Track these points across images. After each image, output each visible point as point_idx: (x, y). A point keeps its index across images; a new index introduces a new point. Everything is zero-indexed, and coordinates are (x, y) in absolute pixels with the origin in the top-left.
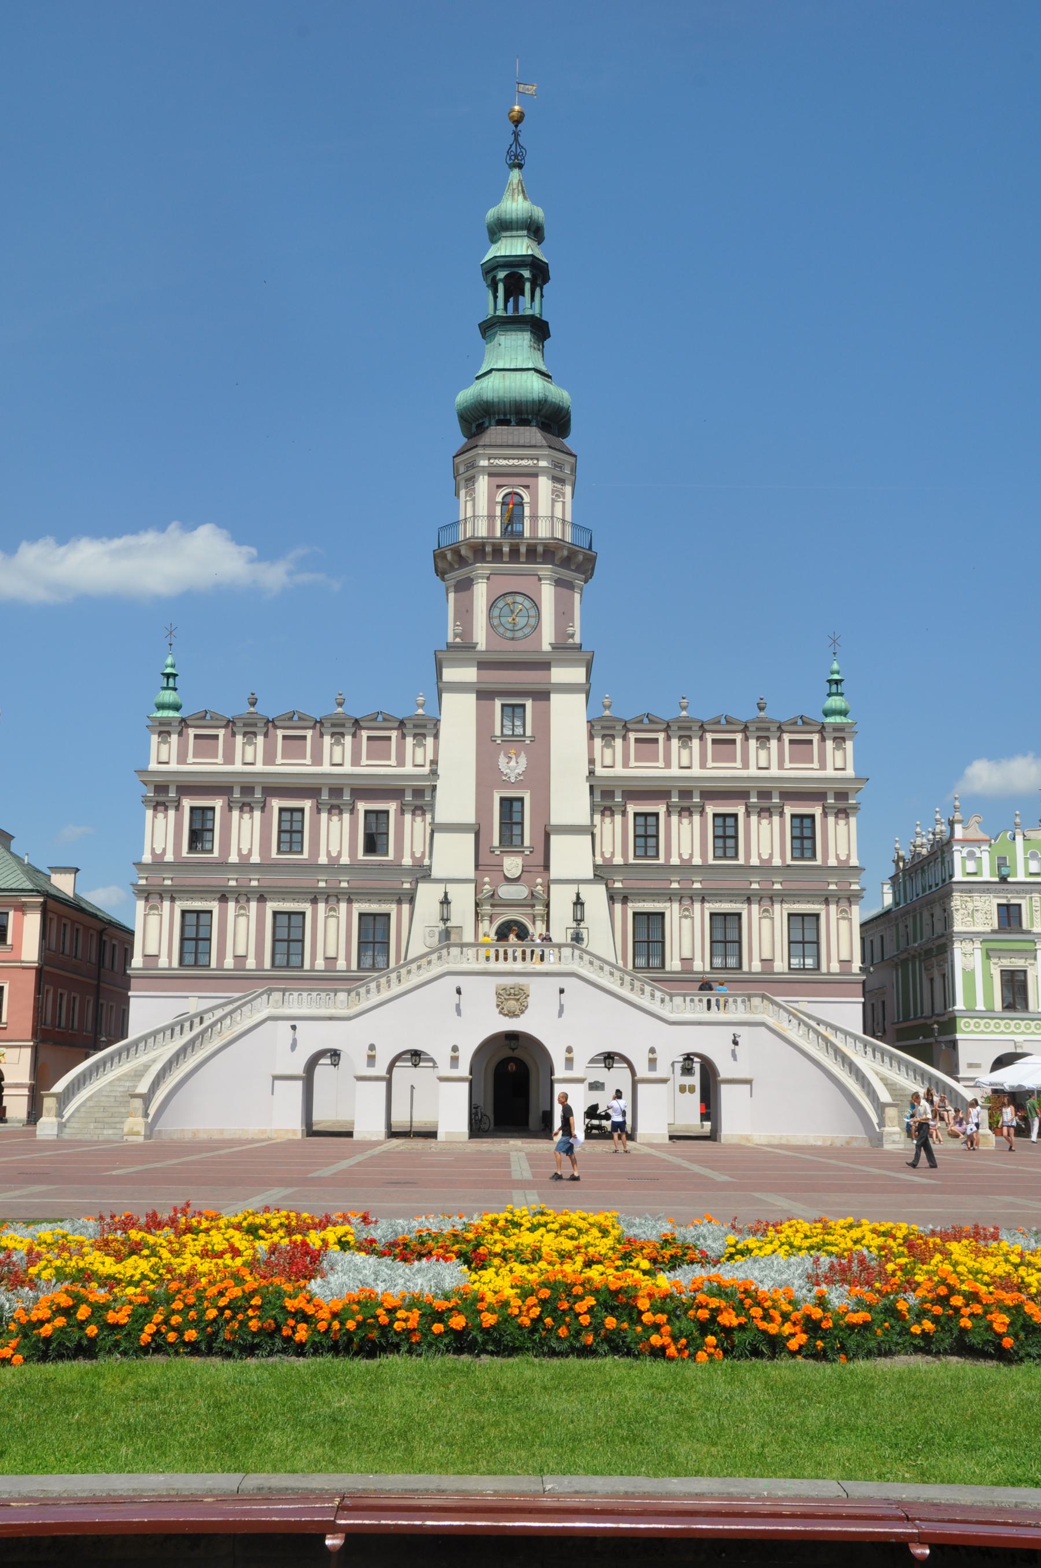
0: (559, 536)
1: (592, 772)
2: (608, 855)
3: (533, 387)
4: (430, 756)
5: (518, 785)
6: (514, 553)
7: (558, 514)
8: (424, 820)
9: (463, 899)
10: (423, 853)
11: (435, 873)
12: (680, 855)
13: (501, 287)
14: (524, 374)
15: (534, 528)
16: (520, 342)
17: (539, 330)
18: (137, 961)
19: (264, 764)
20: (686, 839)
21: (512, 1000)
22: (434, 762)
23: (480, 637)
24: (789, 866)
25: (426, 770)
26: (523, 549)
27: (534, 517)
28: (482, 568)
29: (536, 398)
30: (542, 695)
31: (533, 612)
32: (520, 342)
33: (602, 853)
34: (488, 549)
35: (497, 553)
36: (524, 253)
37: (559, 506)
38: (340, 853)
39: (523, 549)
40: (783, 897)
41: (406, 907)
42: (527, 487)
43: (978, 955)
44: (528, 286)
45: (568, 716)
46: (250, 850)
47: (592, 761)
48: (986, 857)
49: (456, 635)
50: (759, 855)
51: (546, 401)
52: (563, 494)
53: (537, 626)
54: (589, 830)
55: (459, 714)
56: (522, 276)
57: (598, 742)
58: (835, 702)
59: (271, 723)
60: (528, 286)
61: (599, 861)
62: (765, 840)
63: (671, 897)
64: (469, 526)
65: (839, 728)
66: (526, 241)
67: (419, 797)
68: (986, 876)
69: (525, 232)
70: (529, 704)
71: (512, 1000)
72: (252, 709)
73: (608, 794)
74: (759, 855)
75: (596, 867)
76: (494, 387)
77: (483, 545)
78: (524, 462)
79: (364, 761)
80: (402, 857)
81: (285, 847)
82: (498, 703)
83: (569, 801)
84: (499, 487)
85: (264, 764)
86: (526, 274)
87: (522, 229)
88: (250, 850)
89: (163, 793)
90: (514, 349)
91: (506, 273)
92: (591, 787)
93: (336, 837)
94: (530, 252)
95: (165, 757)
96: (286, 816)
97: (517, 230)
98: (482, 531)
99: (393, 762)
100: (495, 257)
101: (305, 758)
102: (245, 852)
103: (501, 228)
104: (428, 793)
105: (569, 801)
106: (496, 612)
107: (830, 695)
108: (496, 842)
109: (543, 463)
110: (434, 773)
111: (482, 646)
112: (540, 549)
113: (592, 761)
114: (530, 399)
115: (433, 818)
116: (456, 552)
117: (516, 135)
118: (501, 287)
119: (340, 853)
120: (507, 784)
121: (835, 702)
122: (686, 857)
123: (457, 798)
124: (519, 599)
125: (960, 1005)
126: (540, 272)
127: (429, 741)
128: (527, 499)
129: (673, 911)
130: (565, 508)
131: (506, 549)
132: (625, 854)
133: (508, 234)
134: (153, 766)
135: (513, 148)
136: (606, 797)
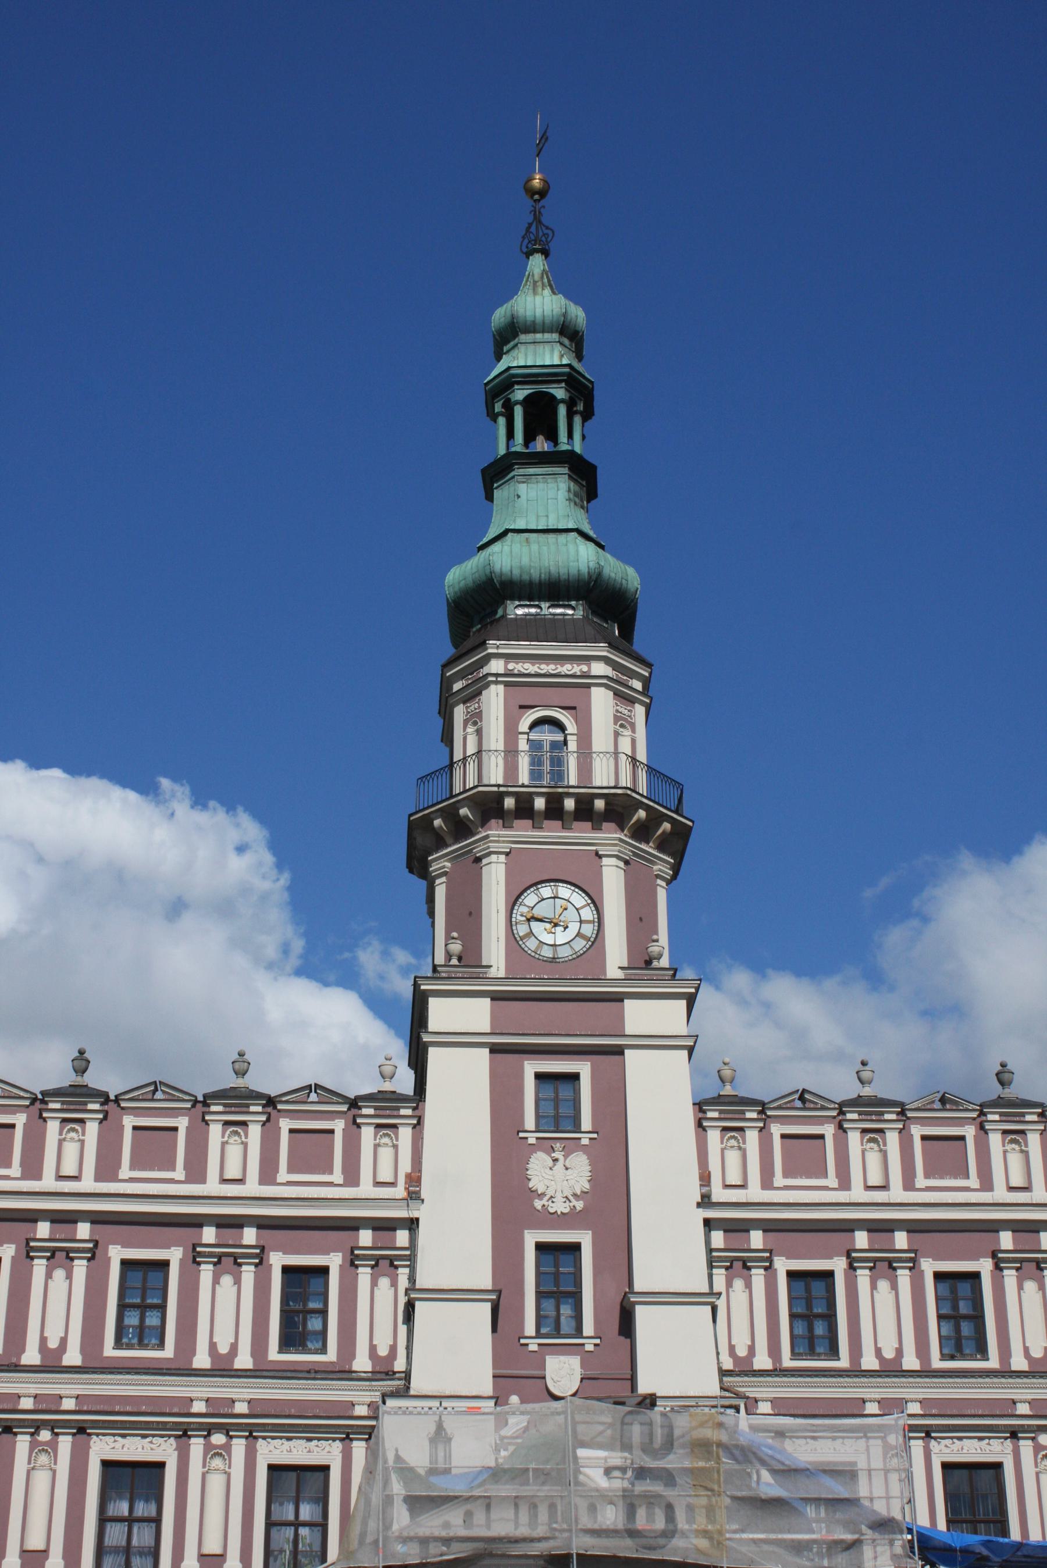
2: (742, 1352)
3: (580, 557)
4: (405, 1166)
6: (555, 811)
8: (394, 1284)
10: (393, 1349)
11: (417, 1385)
12: (878, 1352)
13: (518, 412)
14: (562, 538)
16: (551, 494)
17: (584, 475)
19: (98, 1178)
22: (414, 1179)
23: (495, 954)
25: (400, 1191)
26: (569, 804)
28: (497, 837)
29: (584, 570)
31: (588, 914)
32: (551, 494)
33: (732, 1349)
34: (509, 803)
36: (556, 362)
38: (234, 1348)
39: (569, 804)
41: (359, 1448)
44: (562, 410)
45: (658, 1093)
46: (64, 1341)
47: (705, 1179)
49: (449, 956)
50: (1026, 1350)
51: (600, 574)
54: (709, 1299)
56: (553, 397)
57: (714, 1136)
59: (110, 1104)
60: (562, 410)
61: (728, 1364)
63: (865, 1432)
64: (471, 767)
66: (558, 348)
67: (388, 1241)
69: (555, 336)
70: (584, 1068)
72: (79, 1078)
74: (1026, 1350)
75: (723, 1373)
76: (508, 558)
77: (500, 797)
78: (567, 668)
79: (283, 1176)
80: (353, 1356)
81: (131, 1335)
82: (531, 1067)
84: (524, 707)
85: (98, 1178)
86: (559, 392)
87: (551, 331)
88: (64, 1341)
91: (526, 392)
94: (565, 361)
96: (136, 1278)
98: (495, 774)
99: (337, 1177)
100: (509, 368)
101: (172, 1168)
102: (53, 1344)
104: (402, 1237)
105: (668, 1247)
108: (530, 1328)
109: (599, 669)
110: (414, 1196)
112: (600, 804)
113: (705, 1179)
114: (573, 571)
115: (412, 1279)
116: (450, 813)
118: (518, 412)
119: (234, 1348)
122: (889, 1354)
123: (457, 1242)
124: (564, 891)
126: (582, 393)
127: (405, 1134)
128: (571, 727)
130: (637, 740)
131: (540, 803)
132: (774, 1350)
133: (530, 337)
135: (533, 229)
136: (734, 1239)
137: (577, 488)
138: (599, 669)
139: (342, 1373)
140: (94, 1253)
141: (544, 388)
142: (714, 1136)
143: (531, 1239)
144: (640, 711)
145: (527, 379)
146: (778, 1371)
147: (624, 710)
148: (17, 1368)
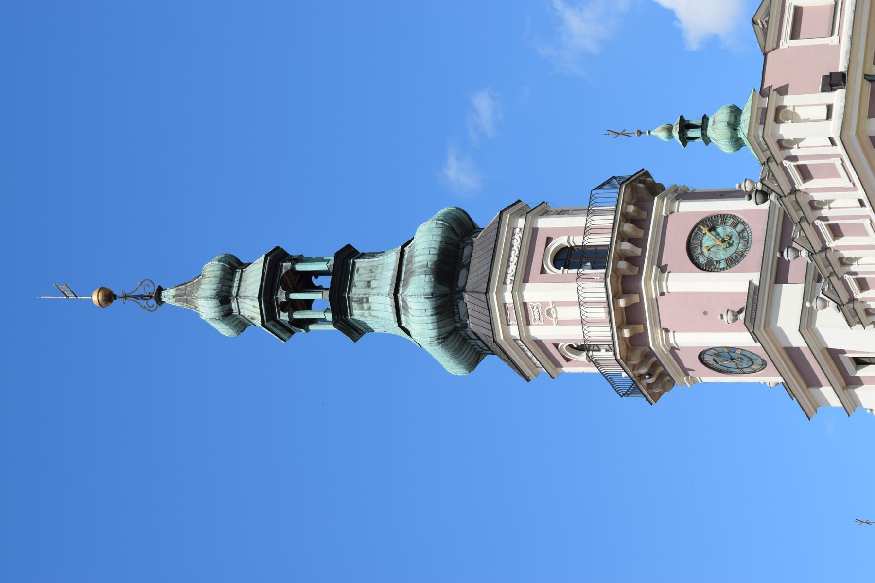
0: (600, 312)
7: (574, 313)
30: (835, 355)
37: (565, 313)
42: (556, 346)
44: (298, 315)
52: (544, 304)
58: (718, 132)
65: (762, 146)
70: (845, 359)
90: (373, 280)
97: (231, 287)
103: (242, 325)
107: (707, 140)
117: (126, 297)
121: (718, 132)
137: (355, 306)
141: (288, 325)
147: (533, 314)
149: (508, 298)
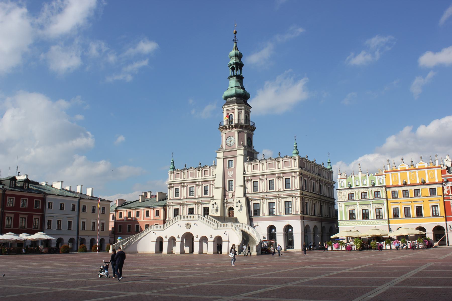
1: (244, 174)
5: (231, 178)
9: (219, 203)
11: (214, 198)
15: (235, 121)
18: (167, 219)
20: (263, 186)
21: (188, 226)
24: (284, 191)
27: (235, 119)
35: (226, 129)
40: (283, 198)
43: (343, 206)
47: (244, 171)
48: (345, 182)
53: (235, 143)
55: (220, 163)
62: (280, 184)
63: (260, 199)
68: (345, 187)
70: (233, 159)
71: (188, 226)
73: (248, 177)
78: (232, 107)
83: (239, 181)
86: (235, 66)
89: (171, 185)
92: (244, 177)
93: (199, 191)
95: (171, 178)
106: (227, 141)
111: (224, 149)
113: (244, 171)
117: (235, 36)
120: (230, 178)
124: (231, 137)
125: (339, 219)
129: (260, 202)
134: (169, 181)
138: (236, 107)
139: (210, 197)
140: (187, 186)
142: (246, 166)
143: (228, 180)
144: (243, 111)
145: (231, 65)
146: (252, 193)
147: (240, 111)
148: (181, 199)
149: (243, 107)
